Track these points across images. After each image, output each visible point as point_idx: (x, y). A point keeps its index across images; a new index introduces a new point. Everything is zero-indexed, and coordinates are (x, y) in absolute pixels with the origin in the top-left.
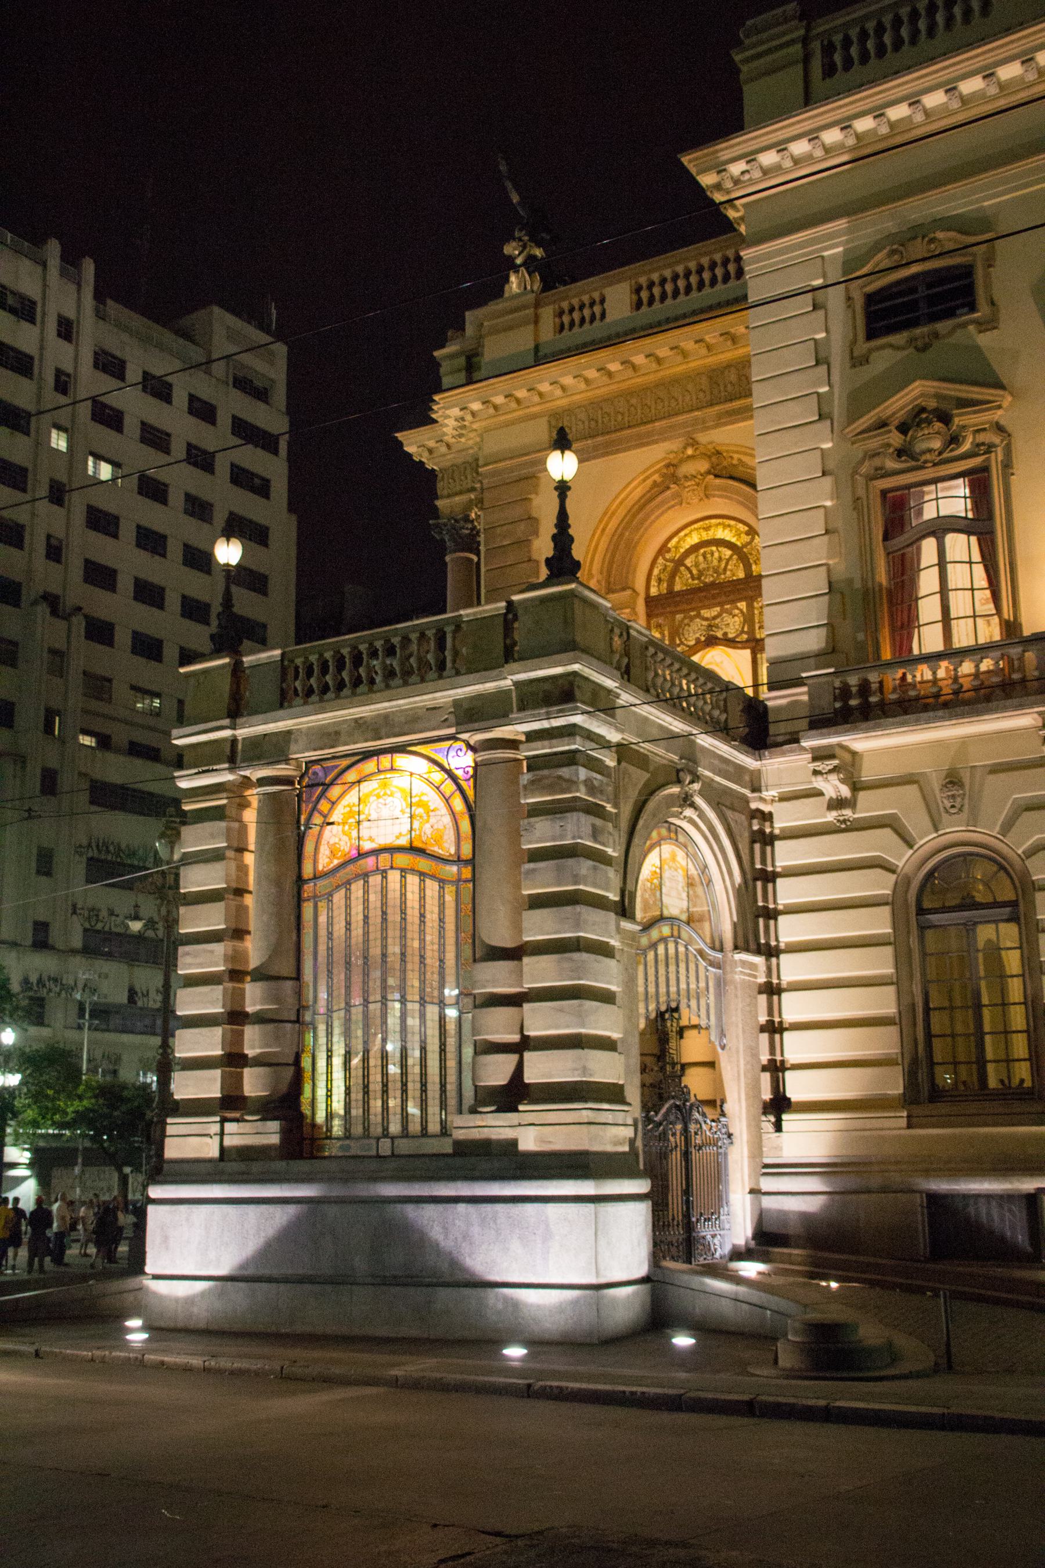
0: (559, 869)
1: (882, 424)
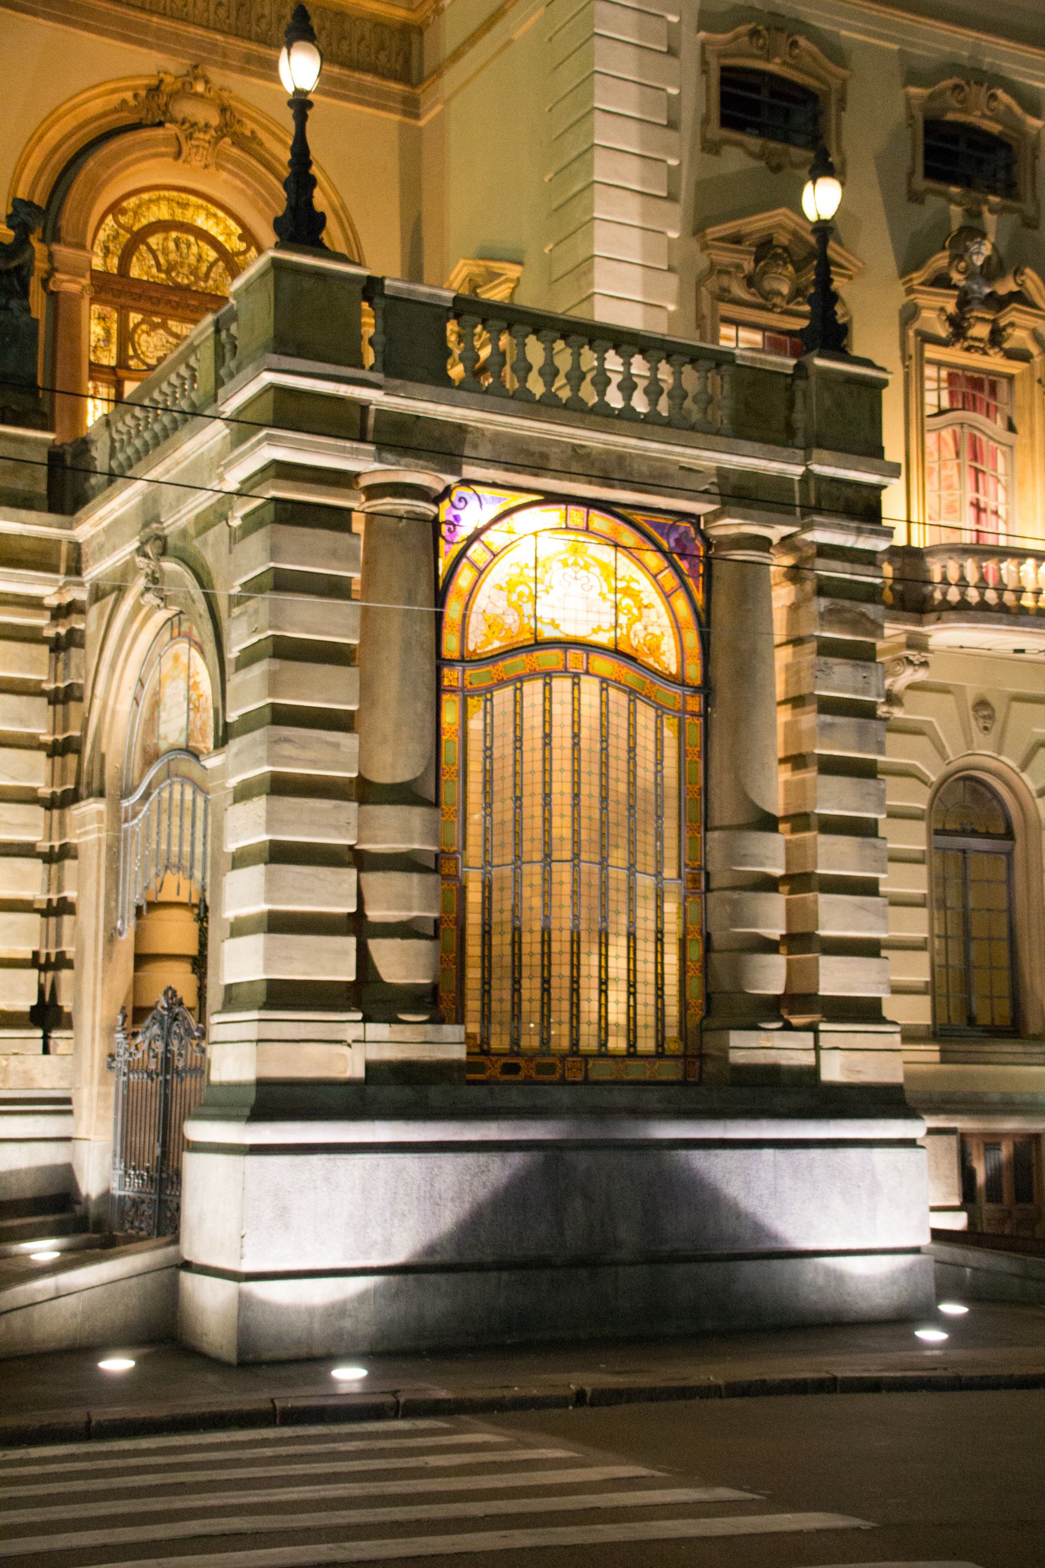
0: (862, 731)
1: (737, 239)
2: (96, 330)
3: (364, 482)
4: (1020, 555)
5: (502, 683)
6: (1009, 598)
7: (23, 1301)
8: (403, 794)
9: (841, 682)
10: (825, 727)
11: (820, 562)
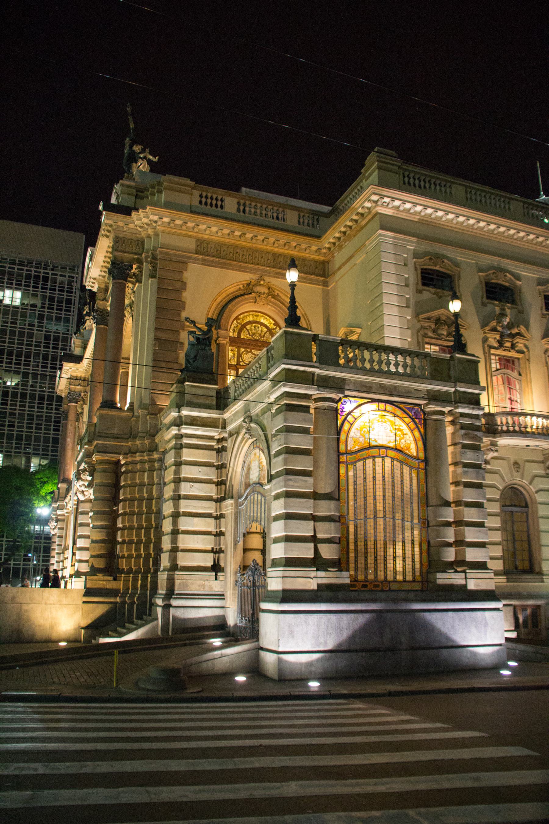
0: (477, 473)
1: (429, 319)
2: (231, 354)
3: (314, 397)
4: (525, 415)
5: (359, 460)
6: (523, 429)
7: (211, 657)
8: (328, 497)
9: (470, 457)
10: (465, 472)
11: (461, 418)
